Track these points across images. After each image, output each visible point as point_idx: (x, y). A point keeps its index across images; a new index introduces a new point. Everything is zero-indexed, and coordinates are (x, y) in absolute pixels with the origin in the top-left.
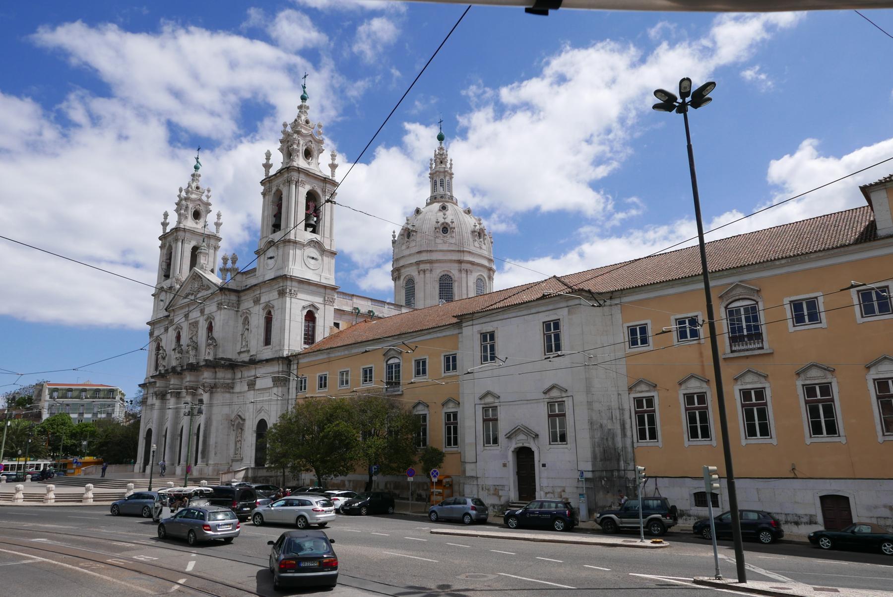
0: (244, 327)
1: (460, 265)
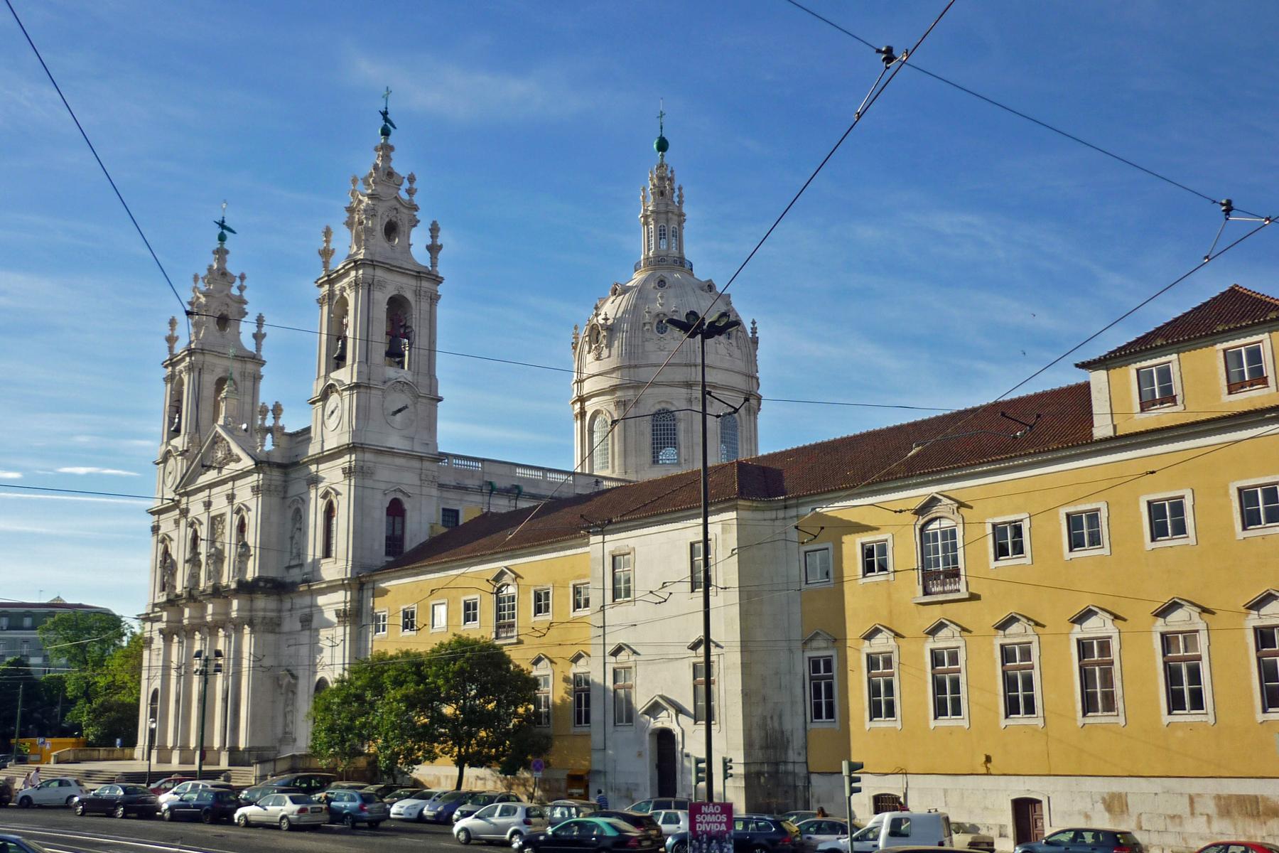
0: (295, 524)
1: (689, 391)
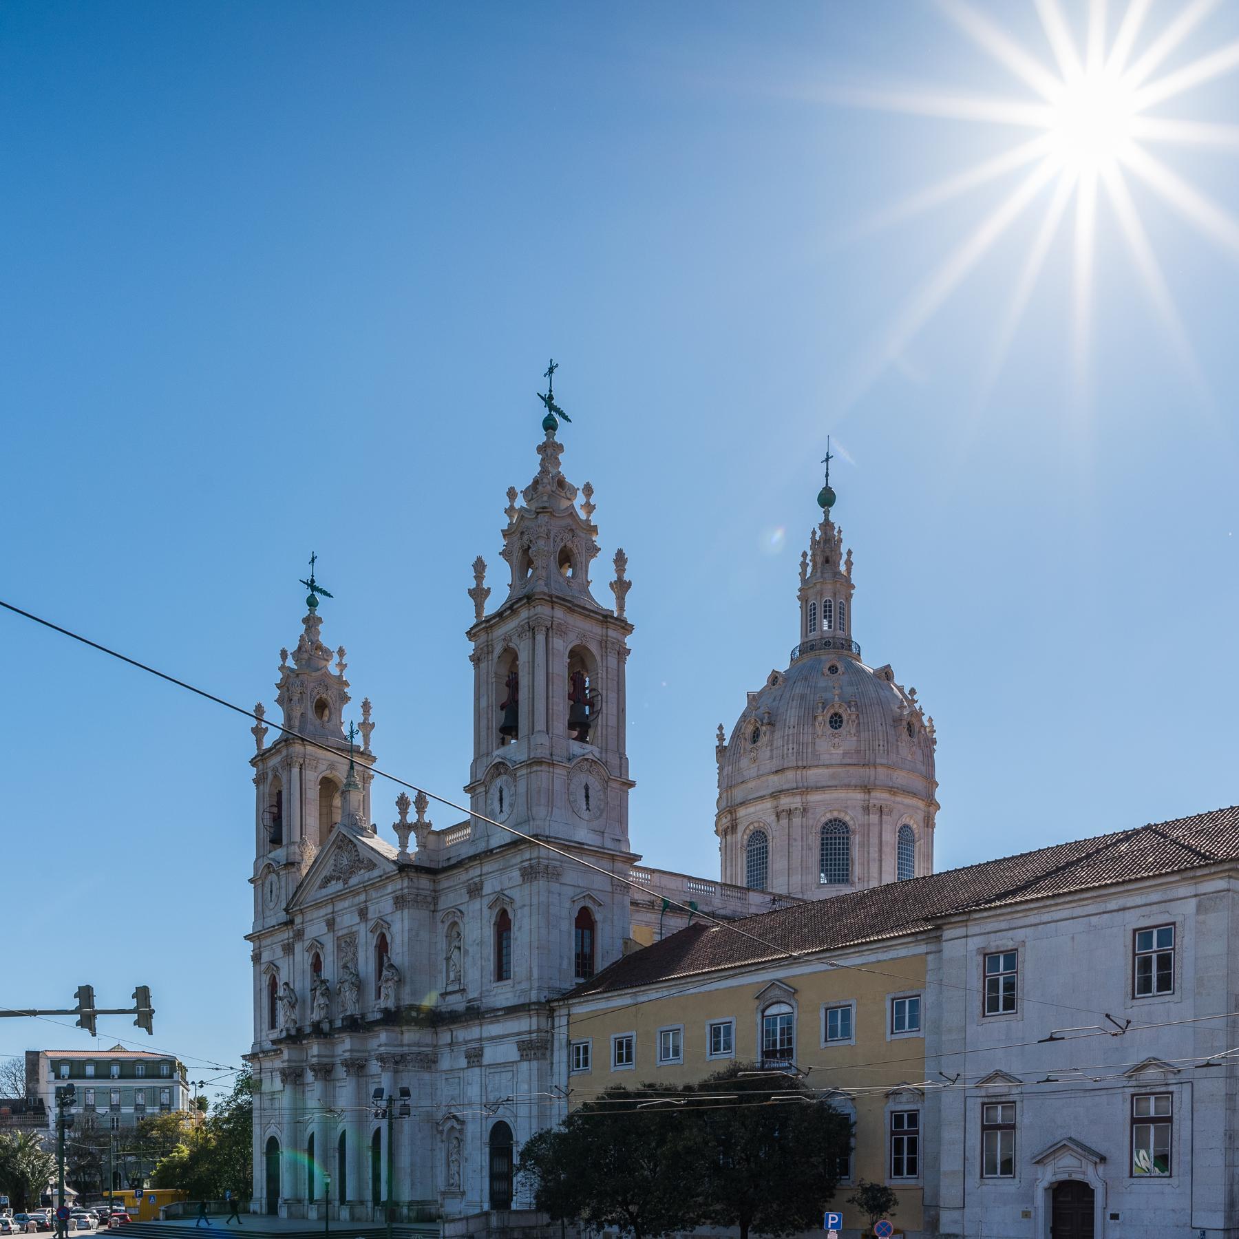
0: (450, 946)
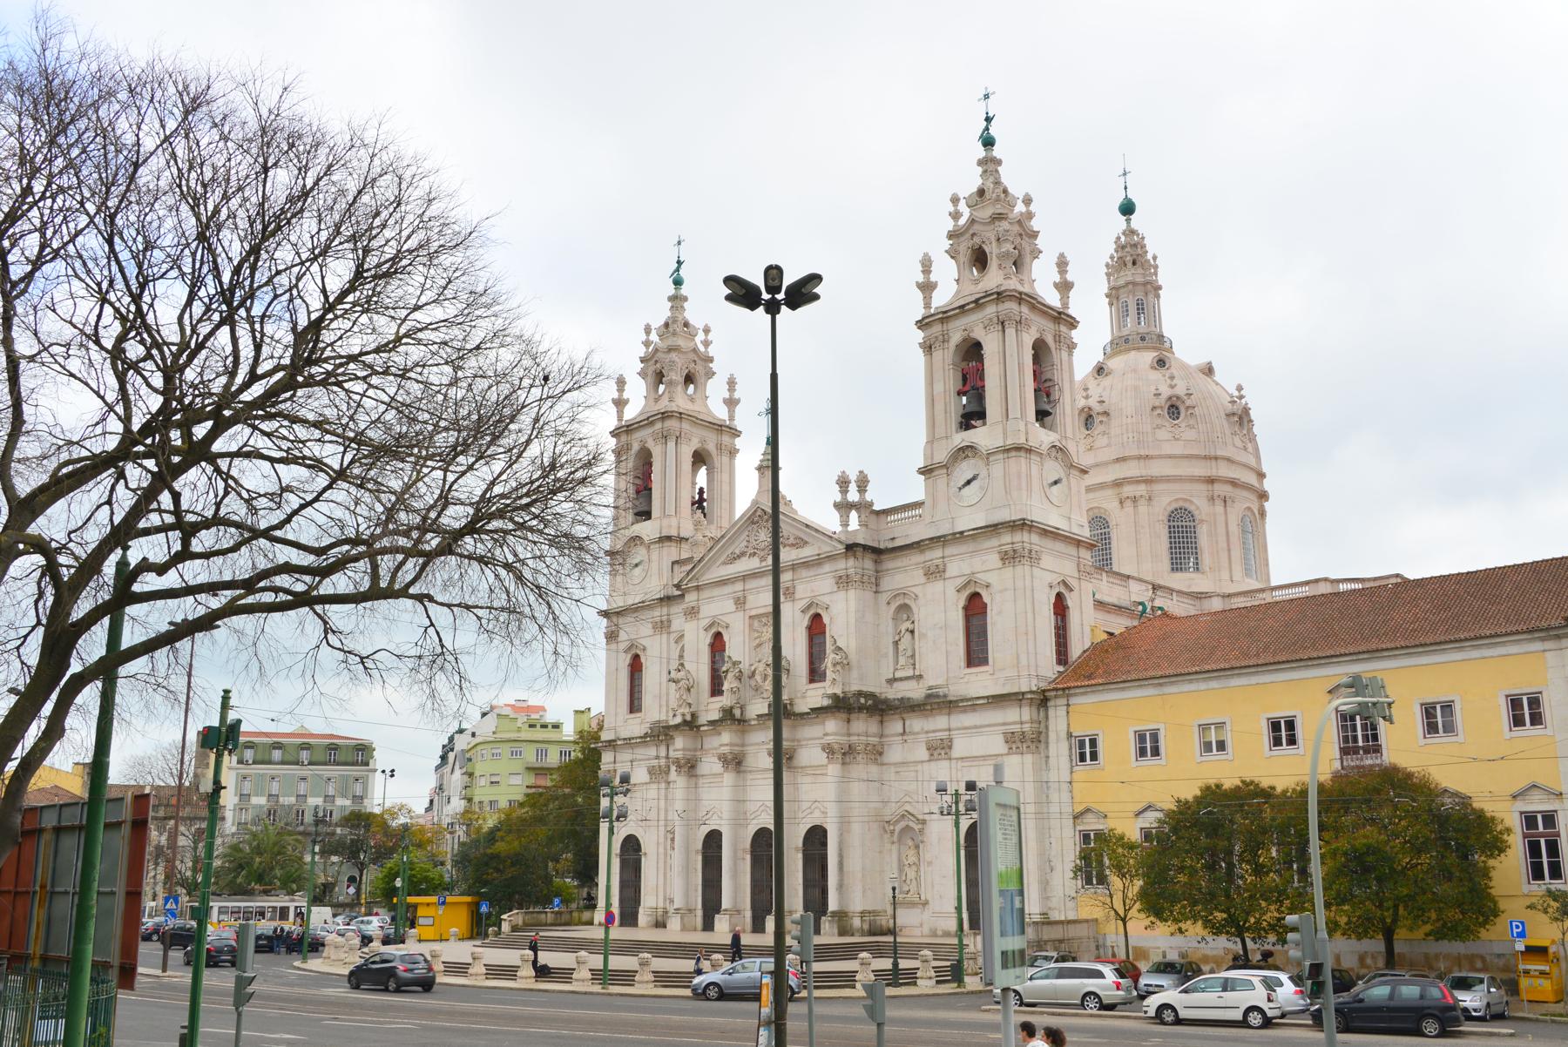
1: (1210, 487)
